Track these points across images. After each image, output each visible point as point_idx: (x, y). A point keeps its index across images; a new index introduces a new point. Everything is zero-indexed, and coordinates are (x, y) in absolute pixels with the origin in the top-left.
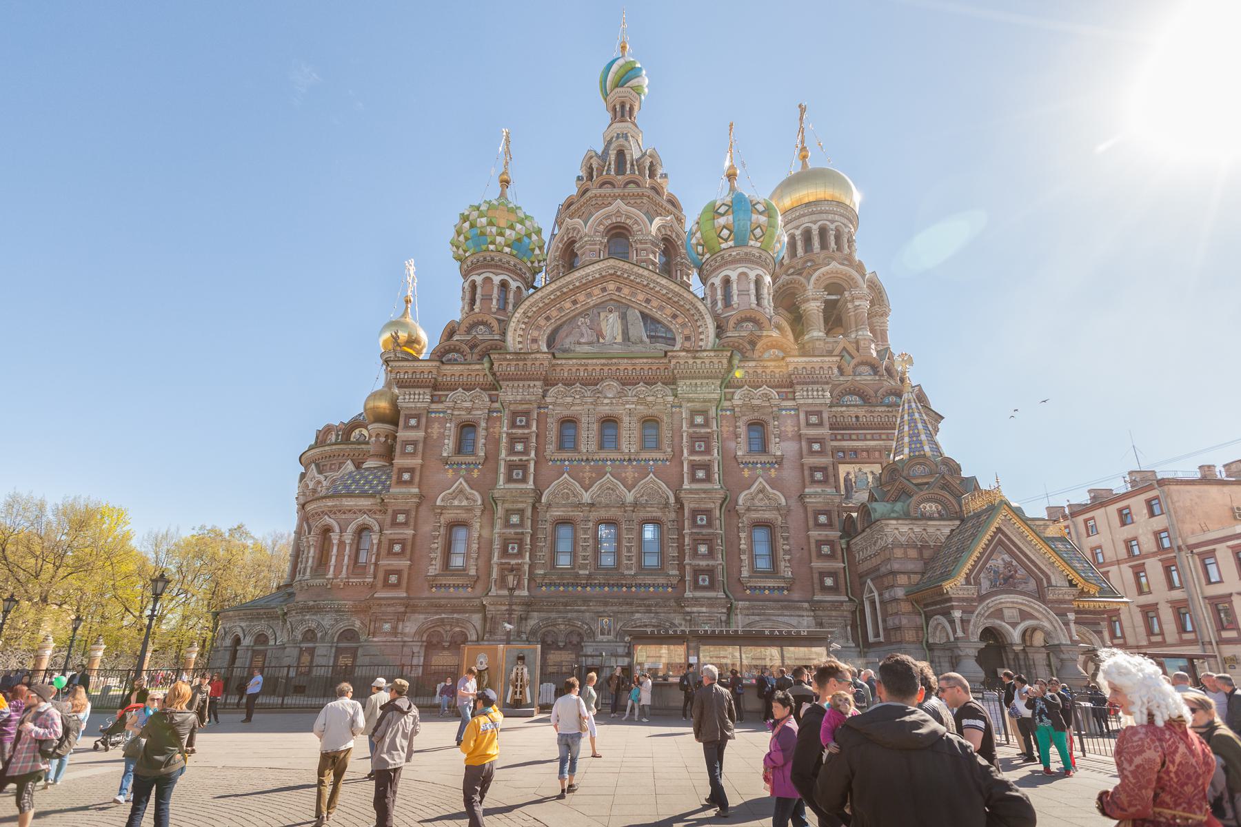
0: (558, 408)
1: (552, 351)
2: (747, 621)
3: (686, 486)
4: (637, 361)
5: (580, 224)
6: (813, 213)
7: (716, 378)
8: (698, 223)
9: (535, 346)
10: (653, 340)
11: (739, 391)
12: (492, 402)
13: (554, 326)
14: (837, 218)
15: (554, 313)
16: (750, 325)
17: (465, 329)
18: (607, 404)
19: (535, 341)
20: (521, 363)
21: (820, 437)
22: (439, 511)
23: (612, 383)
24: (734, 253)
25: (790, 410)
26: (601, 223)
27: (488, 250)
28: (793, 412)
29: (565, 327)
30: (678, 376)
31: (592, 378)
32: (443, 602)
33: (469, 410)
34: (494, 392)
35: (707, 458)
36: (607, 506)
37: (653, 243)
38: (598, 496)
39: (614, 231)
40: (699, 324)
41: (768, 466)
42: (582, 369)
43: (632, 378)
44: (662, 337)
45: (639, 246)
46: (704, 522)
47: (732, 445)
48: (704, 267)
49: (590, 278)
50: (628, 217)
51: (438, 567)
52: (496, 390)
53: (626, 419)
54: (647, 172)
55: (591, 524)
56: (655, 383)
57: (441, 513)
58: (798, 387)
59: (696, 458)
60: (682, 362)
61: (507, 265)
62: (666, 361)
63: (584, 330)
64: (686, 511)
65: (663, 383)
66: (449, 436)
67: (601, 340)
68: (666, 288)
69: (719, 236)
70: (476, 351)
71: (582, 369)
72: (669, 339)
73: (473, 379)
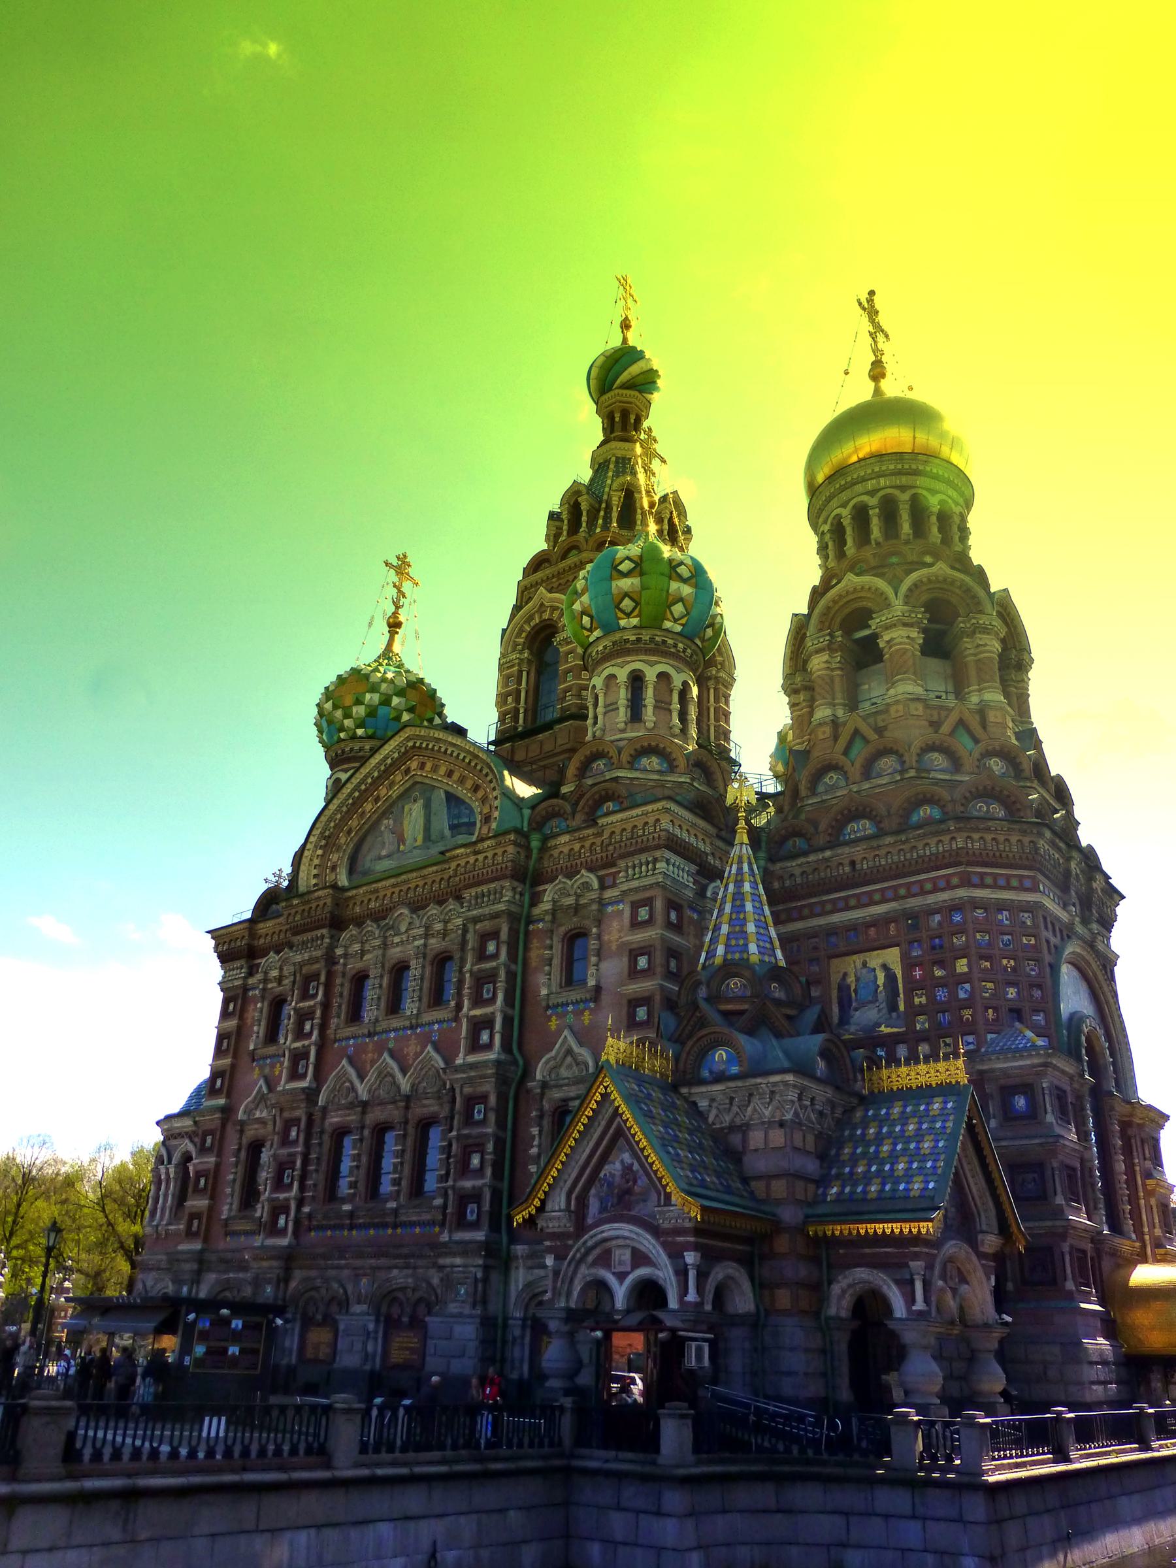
0: (352, 960)
2: (530, 1278)
3: (459, 1061)
4: (425, 872)
6: (843, 489)
13: (356, 839)
14: (882, 481)
20: (307, 907)
21: (647, 943)
22: (239, 1128)
24: (600, 648)
25: (617, 903)
26: (521, 631)
27: (340, 740)
28: (621, 907)
29: (370, 839)
32: (229, 1256)
33: (279, 980)
35: (488, 1010)
36: (382, 1103)
38: (376, 1089)
39: (543, 635)
40: (495, 794)
41: (582, 1006)
42: (373, 897)
46: (482, 1116)
47: (542, 979)
49: (389, 761)
50: (554, 609)
51: (234, 1207)
53: (413, 963)
54: (615, 515)
55: (366, 1132)
57: (242, 1132)
58: (622, 864)
59: (477, 1012)
64: (458, 1099)
66: (259, 1021)
67: (402, 848)
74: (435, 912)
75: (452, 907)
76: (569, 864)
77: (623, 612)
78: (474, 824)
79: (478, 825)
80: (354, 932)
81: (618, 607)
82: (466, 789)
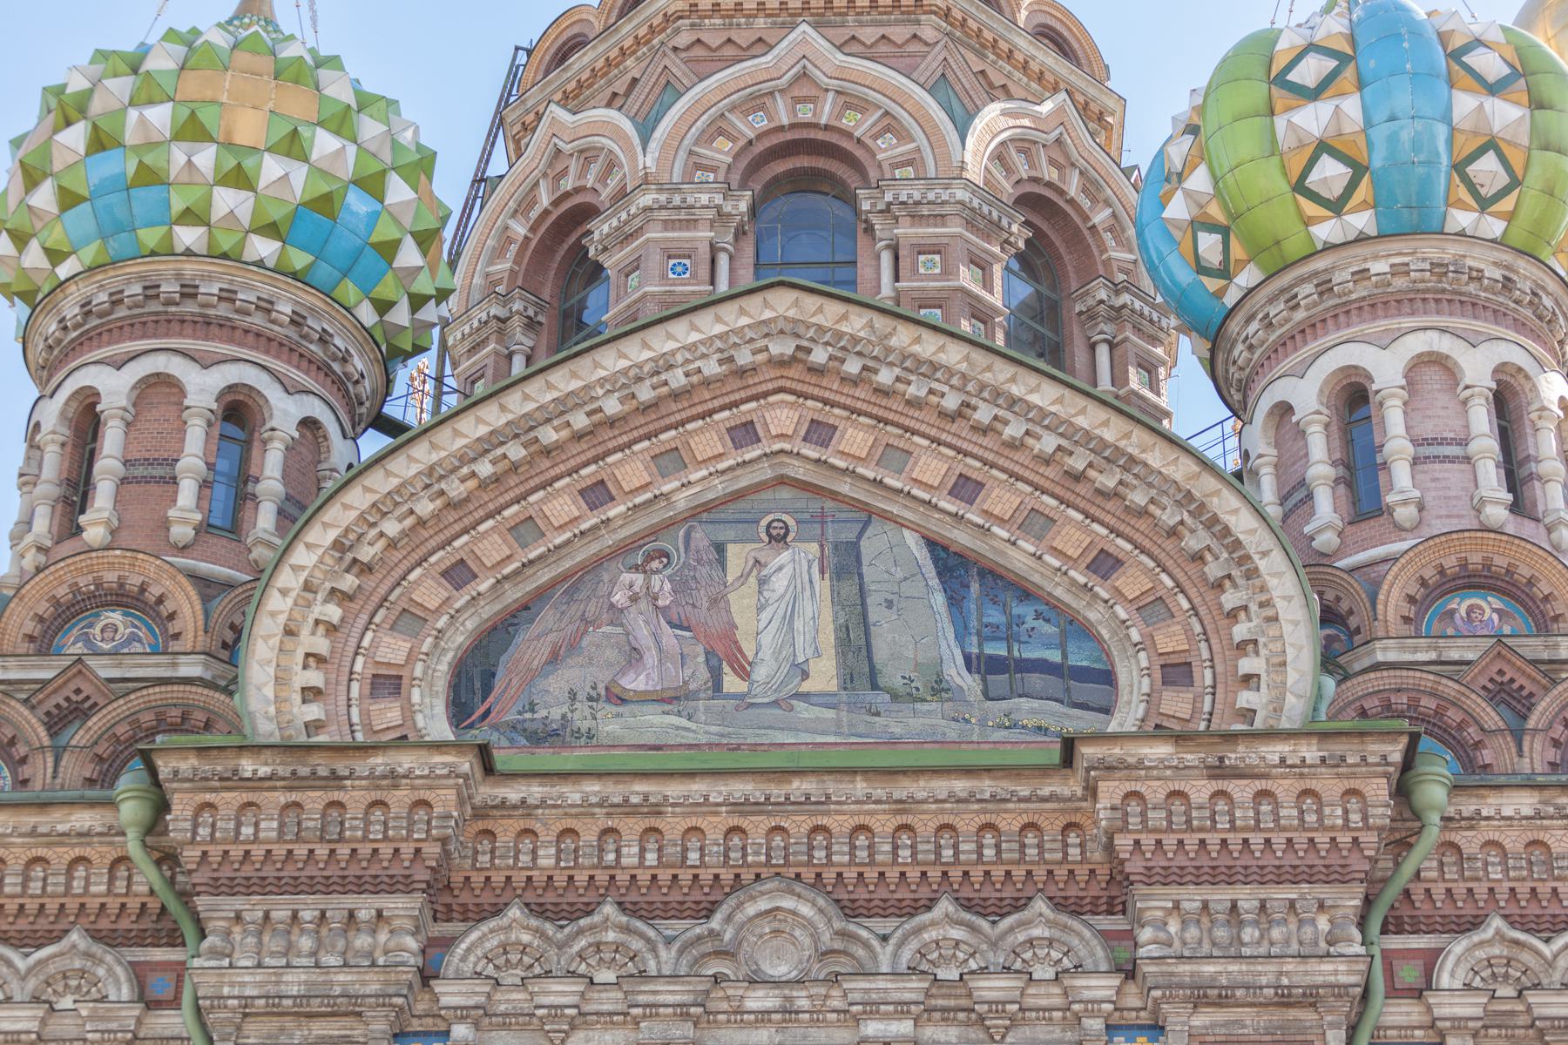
1: (479, 735)
4: (919, 788)
5: (619, 134)
7: (1337, 876)
8: (1193, 130)
9: (388, 714)
10: (999, 681)
11: (1459, 946)
12: (152, 1005)
13: (488, 611)
15: (491, 546)
16: (1488, 606)
17: (30, 627)
18: (763, 1017)
19: (388, 684)
20: (314, 800)
23: (788, 903)
26: (718, 129)
27: (166, 250)
29: (547, 617)
30: (1134, 866)
31: (685, 876)
34: (159, 954)
37: (973, 219)
40: (1230, 599)
42: (631, 827)
43: (892, 874)
44: (1043, 666)
45: (906, 231)
48: (1234, 326)
49: (677, 379)
50: (851, 102)
52: (174, 939)
56: (1019, 905)
60: (1155, 791)
61: (258, 320)
62: (1071, 786)
63: (643, 635)
65: (1059, 904)
67: (731, 683)
68: (1057, 425)
69: (1300, 187)
70: (80, 736)
71: (631, 827)
72: (1081, 674)
73: (57, 883)
74: (957, 933)
75: (1037, 932)
76: (1523, 889)
77: (1472, 188)
78: (1107, 677)
79: (1134, 678)
80: (526, 938)
81: (1459, 167)
82: (1055, 551)
